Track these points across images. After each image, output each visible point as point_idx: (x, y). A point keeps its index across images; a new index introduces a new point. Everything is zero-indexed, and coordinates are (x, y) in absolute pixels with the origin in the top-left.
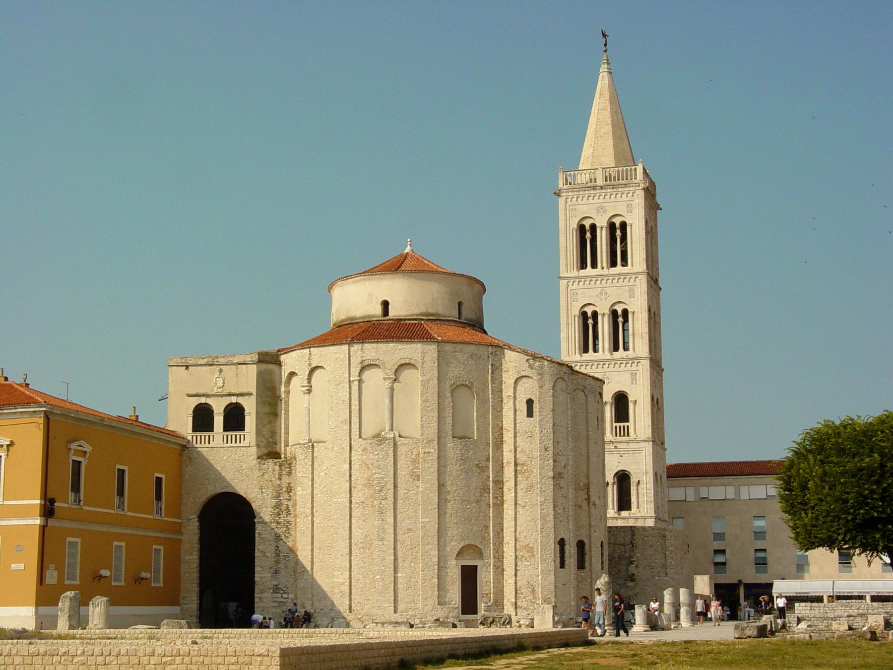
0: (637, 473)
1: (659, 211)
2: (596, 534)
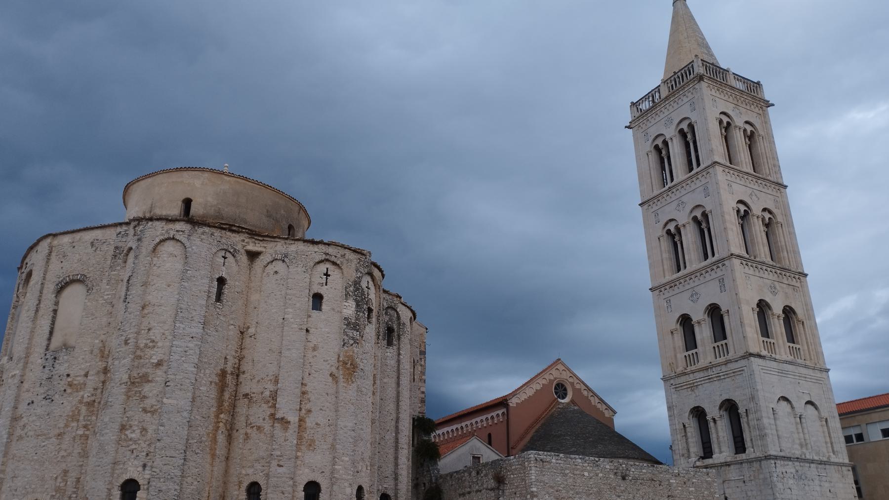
2: (280, 470)
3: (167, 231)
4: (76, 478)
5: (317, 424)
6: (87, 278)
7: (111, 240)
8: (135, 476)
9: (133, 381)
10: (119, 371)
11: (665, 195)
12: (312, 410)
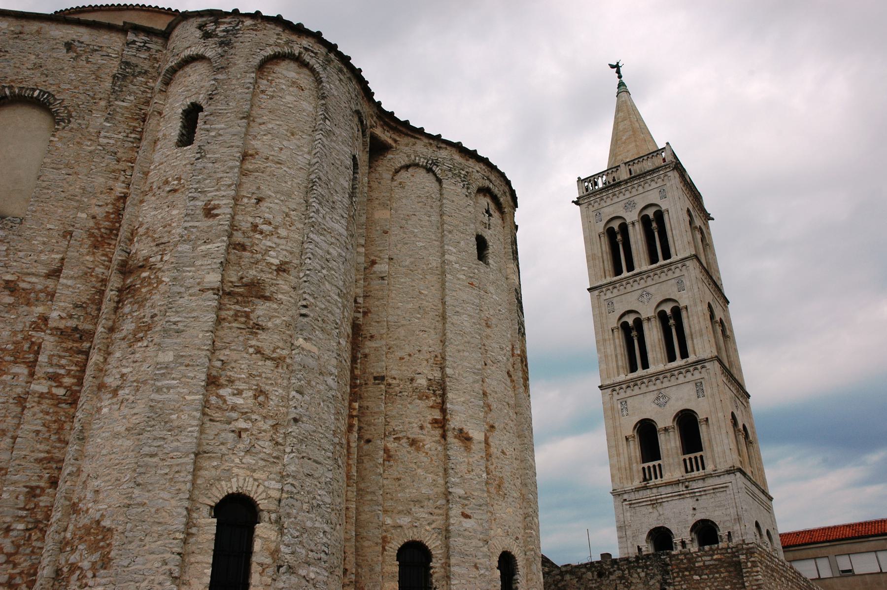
0: (724, 522)
1: (710, 222)
2: (468, 524)
3: (287, 43)
4: (26, 487)
5: (503, 452)
6: (55, 100)
7: (110, 51)
8: (250, 489)
9: (227, 290)
10: (193, 265)
11: (624, 283)
12: (496, 425)
